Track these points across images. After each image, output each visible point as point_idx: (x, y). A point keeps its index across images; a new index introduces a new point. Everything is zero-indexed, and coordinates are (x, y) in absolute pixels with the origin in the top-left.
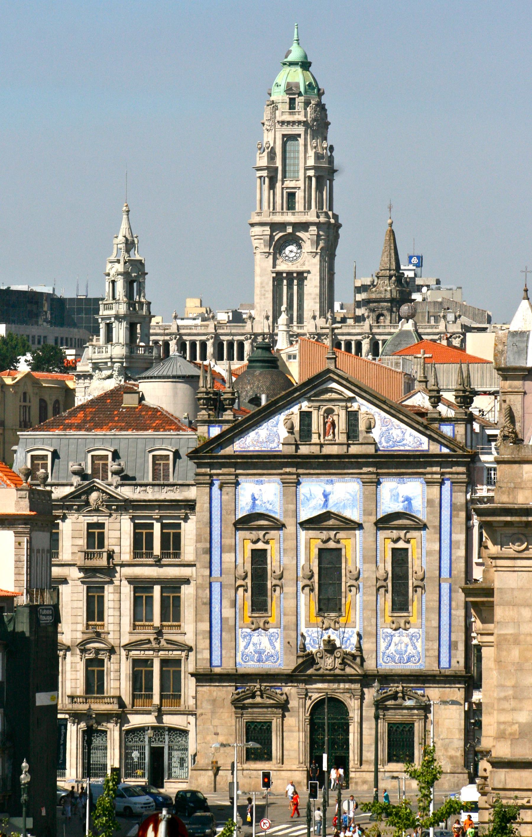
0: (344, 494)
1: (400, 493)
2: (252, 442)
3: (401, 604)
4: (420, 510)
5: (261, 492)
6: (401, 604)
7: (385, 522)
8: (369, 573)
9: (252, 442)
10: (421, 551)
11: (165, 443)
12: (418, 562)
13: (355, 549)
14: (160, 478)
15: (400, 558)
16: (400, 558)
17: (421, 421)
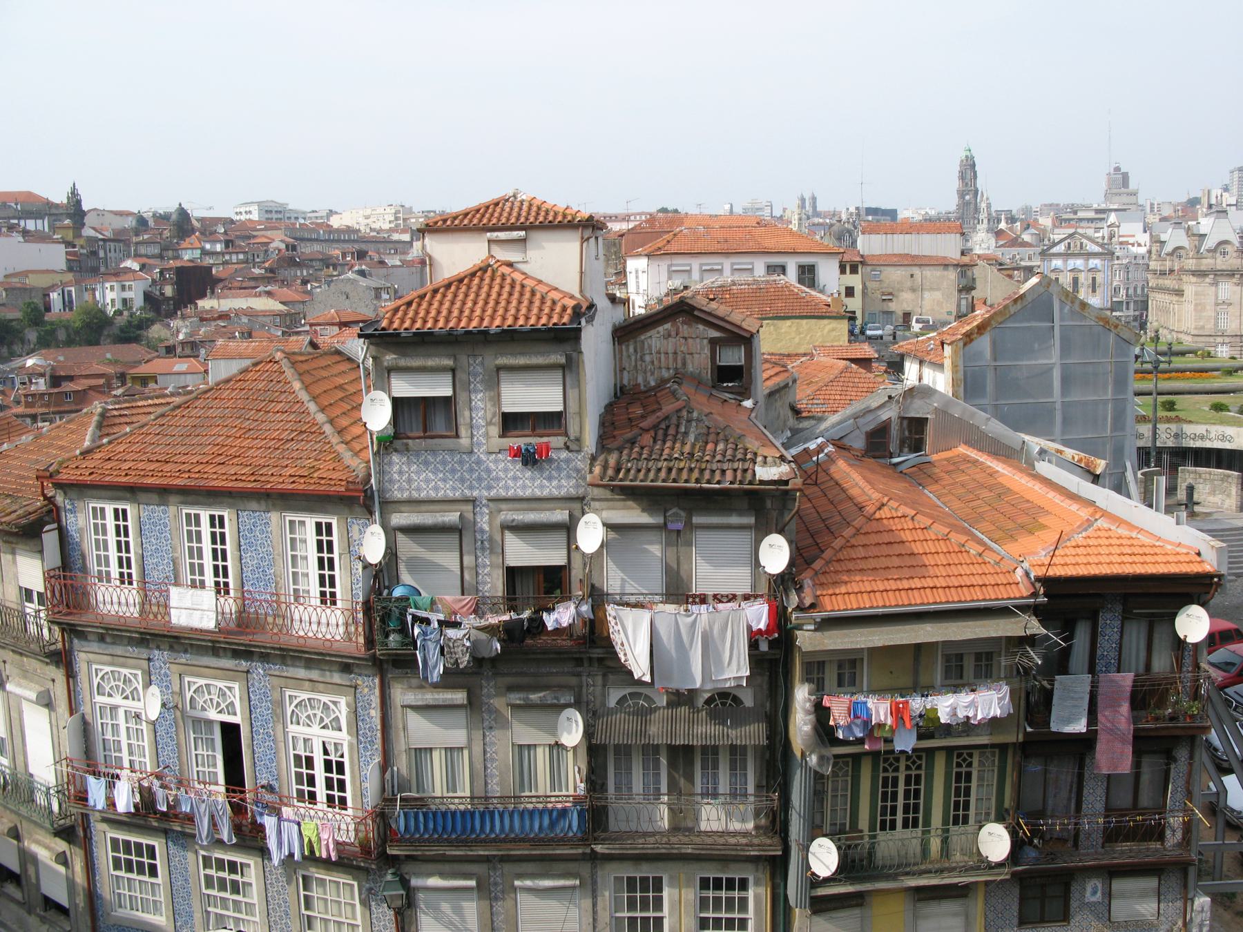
0: (1079, 263)
1: (1094, 262)
2: (1054, 250)
3: (1094, 291)
4: (1099, 267)
5: (1057, 263)
6: (1094, 291)
7: (1090, 270)
8: (1086, 283)
9: (1054, 250)
10: (1100, 278)
11: (1031, 251)
12: (1099, 280)
13: (1082, 277)
14: (1030, 259)
15: (1094, 279)
16: (1094, 279)
17: (1102, 246)
